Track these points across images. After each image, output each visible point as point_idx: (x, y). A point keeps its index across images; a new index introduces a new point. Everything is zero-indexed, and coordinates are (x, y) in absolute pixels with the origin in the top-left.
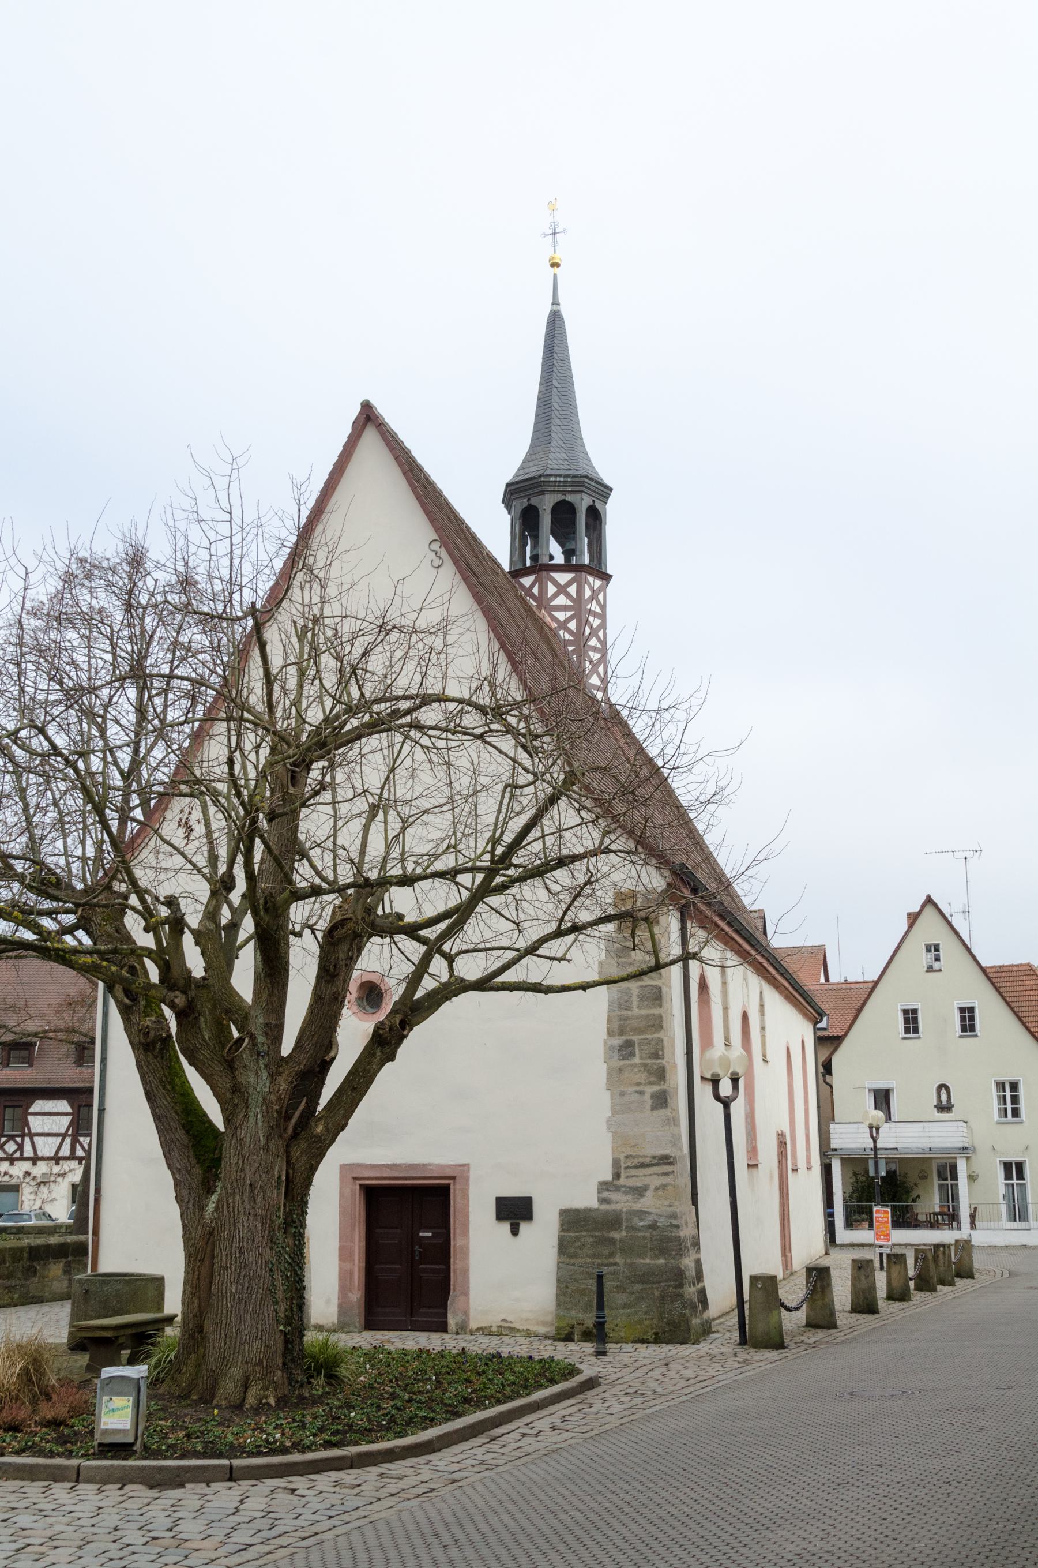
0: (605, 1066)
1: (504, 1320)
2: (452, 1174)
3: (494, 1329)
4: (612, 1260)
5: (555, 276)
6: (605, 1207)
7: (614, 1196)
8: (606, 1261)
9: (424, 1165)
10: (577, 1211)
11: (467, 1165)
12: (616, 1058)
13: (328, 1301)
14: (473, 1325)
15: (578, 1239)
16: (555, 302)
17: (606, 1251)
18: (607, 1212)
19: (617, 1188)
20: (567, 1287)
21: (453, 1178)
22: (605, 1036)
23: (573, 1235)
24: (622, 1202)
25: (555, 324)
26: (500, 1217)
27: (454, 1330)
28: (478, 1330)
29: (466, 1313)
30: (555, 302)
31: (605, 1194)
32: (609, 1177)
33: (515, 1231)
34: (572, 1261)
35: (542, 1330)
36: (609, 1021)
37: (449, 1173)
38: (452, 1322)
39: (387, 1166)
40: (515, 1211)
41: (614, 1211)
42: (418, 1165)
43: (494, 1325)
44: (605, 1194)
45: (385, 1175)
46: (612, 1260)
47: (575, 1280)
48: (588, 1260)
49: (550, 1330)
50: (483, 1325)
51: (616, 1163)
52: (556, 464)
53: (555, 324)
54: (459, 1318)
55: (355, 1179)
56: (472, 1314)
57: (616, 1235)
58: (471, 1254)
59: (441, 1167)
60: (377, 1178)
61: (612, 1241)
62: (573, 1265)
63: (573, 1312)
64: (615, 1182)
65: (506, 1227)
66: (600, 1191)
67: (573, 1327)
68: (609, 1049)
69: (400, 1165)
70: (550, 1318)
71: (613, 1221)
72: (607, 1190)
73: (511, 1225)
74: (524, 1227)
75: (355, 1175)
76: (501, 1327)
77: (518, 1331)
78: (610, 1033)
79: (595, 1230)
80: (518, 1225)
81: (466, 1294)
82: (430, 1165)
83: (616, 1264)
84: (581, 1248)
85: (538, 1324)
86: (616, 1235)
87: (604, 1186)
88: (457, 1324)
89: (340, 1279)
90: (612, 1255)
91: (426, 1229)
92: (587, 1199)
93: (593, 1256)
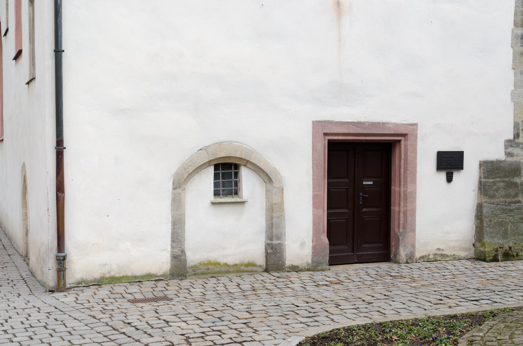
0: (511, 50)
1: (439, 249)
2: (404, 132)
3: (431, 257)
4: (516, 199)
6: (510, 159)
7: (516, 151)
8: (513, 200)
9: (383, 123)
10: (492, 162)
11: (416, 125)
12: (519, 44)
13: (303, 244)
14: (418, 255)
15: (494, 183)
17: (512, 191)
18: (511, 163)
19: (518, 145)
20: (491, 221)
21: (404, 135)
22: (512, 26)
23: (491, 180)
24: (522, 156)
26: (440, 167)
27: (405, 261)
28: (422, 257)
29: (413, 246)
31: (510, 150)
32: (511, 137)
33: (449, 179)
34: (492, 200)
35: (463, 254)
36: (515, 15)
37: (402, 131)
38: (403, 253)
39: (354, 123)
40: (450, 163)
41: (515, 162)
42: (378, 123)
43: (431, 253)
44: (510, 150)
45: (352, 131)
46: (516, 199)
47: (496, 215)
48: (502, 200)
49: (471, 253)
50: (424, 254)
51: (516, 126)
54: (408, 251)
55: (325, 134)
57: (517, 180)
58: (417, 198)
59: (396, 125)
61: (515, 185)
62: (493, 203)
63: (496, 239)
64: (516, 141)
65: (443, 176)
66: (506, 147)
67: (497, 251)
68: (515, 37)
69: (364, 123)
70: (469, 245)
71: (514, 170)
72: (511, 146)
73: (448, 174)
74: (456, 176)
75: (326, 132)
76: (435, 254)
77: (447, 256)
78: (516, 24)
79: (505, 176)
80: (452, 173)
81: (414, 231)
82: (388, 123)
83: (519, 202)
84: (497, 190)
85: (460, 250)
86: (517, 180)
87: (509, 144)
88: (407, 255)
89: (314, 224)
90: (516, 195)
91: (369, 178)
92: (497, 153)
93: (507, 196)
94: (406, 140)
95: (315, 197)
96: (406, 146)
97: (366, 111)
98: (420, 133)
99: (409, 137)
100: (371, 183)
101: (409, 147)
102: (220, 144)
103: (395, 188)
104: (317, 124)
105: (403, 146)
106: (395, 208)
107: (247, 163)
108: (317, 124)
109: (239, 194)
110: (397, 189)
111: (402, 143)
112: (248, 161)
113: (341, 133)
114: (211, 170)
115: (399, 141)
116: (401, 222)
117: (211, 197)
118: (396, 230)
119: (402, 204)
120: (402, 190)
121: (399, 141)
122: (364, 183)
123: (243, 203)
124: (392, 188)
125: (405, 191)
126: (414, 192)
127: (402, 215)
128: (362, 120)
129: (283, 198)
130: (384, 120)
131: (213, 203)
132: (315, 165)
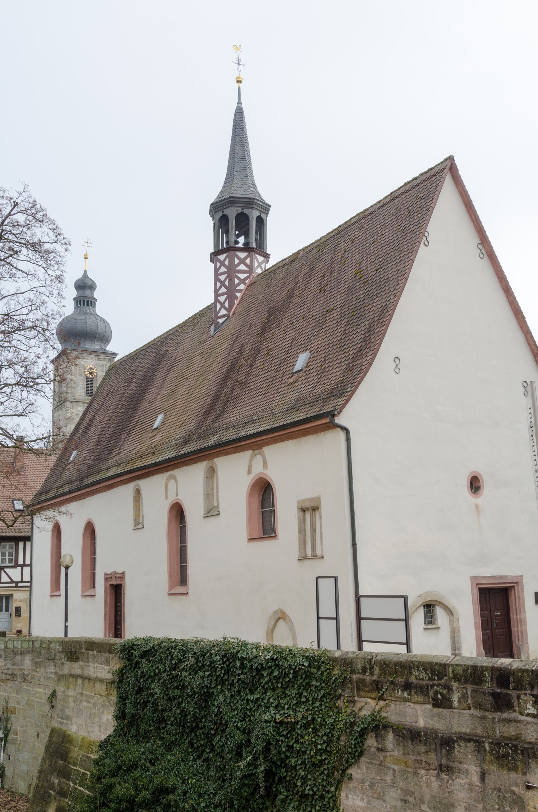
5: (239, 88)
9: (506, 576)
11: (522, 576)
16: (239, 102)
21: (517, 583)
25: (239, 114)
29: (528, 653)
30: (239, 102)
37: (516, 580)
42: (503, 576)
52: (237, 192)
53: (239, 114)
55: (477, 584)
56: (530, 653)
60: (491, 584)
81: (527, 643)
82: (508, 576)
89: (476, 640)
91: (497, 611)
94: (518, 586)
95: (476, 623)
96: (518, 589)
97: (496, 570)
98: (524, 581)
99: (520, 584)
100: (499, 613)
101: (520, 590)
102: (427, 593)
103: (513, 616)
104: (473, 578)
105: (516, 589)
106: (514, 629)
107: (440, 604)
108: (473, 578)
109: (435, 623)
110: (515, 617)
111: (516, 587)
112: (440, 603)
113: (486, 584)
114: (423, 607)
115: (514, 587)
116: (520, 638)
117: (423, 626)
118: (517, 643)
119: (519, 626)
120: (518, 617)
121: (514, 587)
122: (496, 614)
123: (439, 628)
124: (511, 616)
125: (520, 618)
126: (525, 618)
127: (520, 633)
128: (495, 575)
129: (459, 624)
130: (506, 574)
131: (425, 629)
132: (474, 604)
